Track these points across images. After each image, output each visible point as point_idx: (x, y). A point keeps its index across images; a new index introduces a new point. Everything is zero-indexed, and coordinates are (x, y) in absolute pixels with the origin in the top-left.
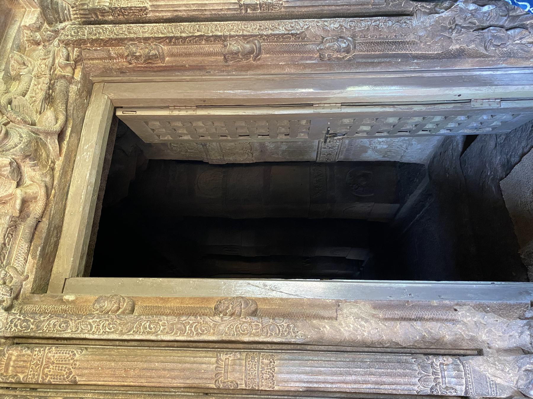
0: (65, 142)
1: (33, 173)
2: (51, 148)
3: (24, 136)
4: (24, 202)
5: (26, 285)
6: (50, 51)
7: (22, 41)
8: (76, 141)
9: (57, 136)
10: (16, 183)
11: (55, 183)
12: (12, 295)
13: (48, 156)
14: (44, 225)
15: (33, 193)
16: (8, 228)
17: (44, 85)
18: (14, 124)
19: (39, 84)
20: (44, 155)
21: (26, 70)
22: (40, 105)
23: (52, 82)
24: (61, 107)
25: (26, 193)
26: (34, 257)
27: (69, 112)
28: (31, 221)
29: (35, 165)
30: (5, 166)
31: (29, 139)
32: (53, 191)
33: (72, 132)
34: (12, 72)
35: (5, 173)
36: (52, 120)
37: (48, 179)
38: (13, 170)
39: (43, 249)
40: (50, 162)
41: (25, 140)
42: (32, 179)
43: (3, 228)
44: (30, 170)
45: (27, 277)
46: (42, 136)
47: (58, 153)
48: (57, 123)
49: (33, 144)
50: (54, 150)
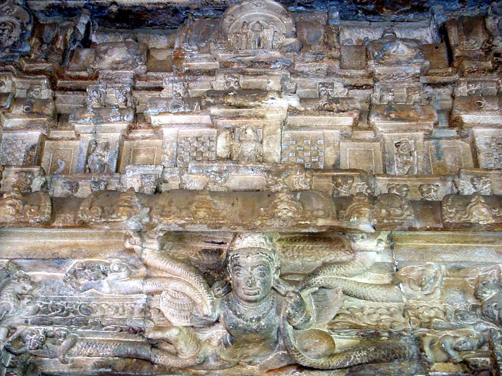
1: (215, 343)
2: (271, 357)
3: (263, 323)
5: (55, 363)
6: (463, 319)
7: (474, 270)
9: (293, 362)
10: (189, 324)
12: (33, 351)
13: (256, 356)
15: (181, 349)
19: (391, 315)
21: (410, 291)
23: (405, 334)
24: (358, 357)
26: (96, 366)
28: (146, 352)
34: (403, 270)
38: (202, 319)
40: (247, 360)
42: (209, 340)
44: (219, 338)
45: (64, 362)
46: (281, 342)
50: (269, 361)
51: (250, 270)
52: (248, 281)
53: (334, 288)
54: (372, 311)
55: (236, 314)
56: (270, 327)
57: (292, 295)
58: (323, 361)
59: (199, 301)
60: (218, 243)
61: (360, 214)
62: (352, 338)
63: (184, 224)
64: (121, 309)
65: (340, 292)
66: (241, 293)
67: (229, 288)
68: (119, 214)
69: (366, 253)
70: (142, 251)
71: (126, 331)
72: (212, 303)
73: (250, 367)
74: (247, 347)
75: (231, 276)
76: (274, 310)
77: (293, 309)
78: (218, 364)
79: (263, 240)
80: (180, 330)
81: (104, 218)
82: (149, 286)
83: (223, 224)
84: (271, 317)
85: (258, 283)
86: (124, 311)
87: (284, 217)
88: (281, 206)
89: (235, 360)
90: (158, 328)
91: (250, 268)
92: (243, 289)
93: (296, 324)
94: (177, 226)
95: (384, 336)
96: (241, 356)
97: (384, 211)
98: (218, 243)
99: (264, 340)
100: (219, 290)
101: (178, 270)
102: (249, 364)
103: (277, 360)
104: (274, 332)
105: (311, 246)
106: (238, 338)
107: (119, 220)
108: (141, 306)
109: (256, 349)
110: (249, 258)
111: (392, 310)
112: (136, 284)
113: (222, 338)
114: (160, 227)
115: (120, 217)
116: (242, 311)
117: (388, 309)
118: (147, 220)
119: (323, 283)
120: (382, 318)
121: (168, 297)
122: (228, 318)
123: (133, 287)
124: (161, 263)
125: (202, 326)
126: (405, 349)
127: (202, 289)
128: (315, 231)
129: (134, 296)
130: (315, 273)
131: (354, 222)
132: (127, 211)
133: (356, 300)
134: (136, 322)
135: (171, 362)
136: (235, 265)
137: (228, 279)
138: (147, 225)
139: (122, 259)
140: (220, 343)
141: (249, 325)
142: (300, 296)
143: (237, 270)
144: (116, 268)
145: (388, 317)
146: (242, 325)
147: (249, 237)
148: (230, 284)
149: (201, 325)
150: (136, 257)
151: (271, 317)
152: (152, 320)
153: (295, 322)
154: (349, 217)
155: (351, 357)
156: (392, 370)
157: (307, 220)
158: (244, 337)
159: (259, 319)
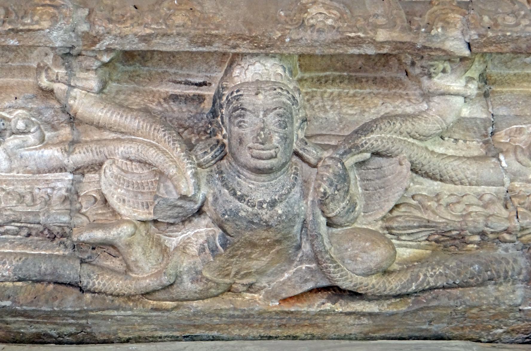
0: (328, 306)
1: (193, 250)
2: (286, 275)
4: (109, 247)
8: (354, 330)
9: (324, 283)
10: (151, 217)
11: (195, 304)
13: (261, 273)
14: (70, 301)
16: (39, 223)
17: (481, 220)
18: (313, 177)
19: (485, 206)
20: (255, 265)
22: (411, 224)
23: (507, 237)
24: (430, 276)
25: (129, 245)
27: (429, 296)
28: (71, 271)
29: (214, 251)
30: (176, 187)
31: (272, 222)
32: (170, 304)
33: (371, 315)
34: (503, 132)
35: (162, 190)
36: (363, 262)
37: (188, 285)
38: (175, 206)
39: (14, 313)
40: (245, 281)
41: (265, 214)
42: (183, 248)
43: (37, 214)
44: (201, 241)
46: (306, 248)
47: (284, 295)
48: (366, 275)
49: (265, 234)
50: (284, 283)
51: (261, 116)
52: (259, 135)
53: (396, 156)
54: (453, 199)
55: (235, 194)
56: (289, 219)
57: (330, 162)
58: (374, 281)
59: (172, 171)
60: (196, 84)
61: (446, 24)
62: (418, 247)
63: (150, 35)
64: (28, 198)
65: (407, 165)
66: (245, 157)
67: (223, 152)
68: (36, 18)
69: (448, 97)
70: (68, 93)
71: (37, 235)
72: (195, 175)
73: (248, 296)
74: (248, 256)
75: (224, 132)
76: (297, 189)
77: (331, 185)
78: (198, 287)
79: (280, 71)
80: (136, 227)
81: (10, 23)
82: (80, 157)
83: (216, 36)
84: (292, 201)
85: (276, 138)
86: (34, 200)
87: (320, 25)
88: (313, 10)
89: (227, 280)
90: (95, 225)
91: (261, 113)
92: (250, 148)
93: (333, 214)
94: (136, 40)
95: (471, 243)
96: (237, 273)
97: (486, 19)
98: (196, 84)
99: (279, 241)
100: (206, 153)
101: (132, 122)
102: (248, 291)
103: (298, 279)
104: (297, 228)
105: (352, 92)
106: (236, 238)
107: (36, 27)
108: (63, 192)
109: (265, 260)
110: (260, 96)
111: (487, 197)
112: (53, 154)
113: (207, 241)
114: (106, 42)
115: (37, 23)
116: (245, 191)
117: (480, 197)
118: (84, 27)
119: (379, 146)
120: (471, 209)
121: (115, 170)
122: (220, 201)
123: (51, 159)
124: (101, 113)
125: (171, 221)
126: (508, 263)
127: (177, 151)
128: (371, 51)
129: (50, 176)
130: (365, 129)
131: (437, 36)
132: (49, 14)
133: (427, 182)
134: (58, 217)
135: (117, 284)
136: (236, 109)
137: (220, 137)
138: (85, 36)
139: (30, 110)
140: (202, 250)
141: (256, 215)
142: (343, 164)
143: (240, 116)
144: (21, 125)
145: (479, 209)
146: (244, 214)
147: (257, 64)
148: (223, 145)
149: (170, 217)
150: (57, 106)
151: (292, 201)
152: (83, 214)
153: (333, 211)
154: (429, 26)
155: (418, 276)
156: (484, 298)
157: (359, 30)
158: (247, 234)
159: (273, 204)
